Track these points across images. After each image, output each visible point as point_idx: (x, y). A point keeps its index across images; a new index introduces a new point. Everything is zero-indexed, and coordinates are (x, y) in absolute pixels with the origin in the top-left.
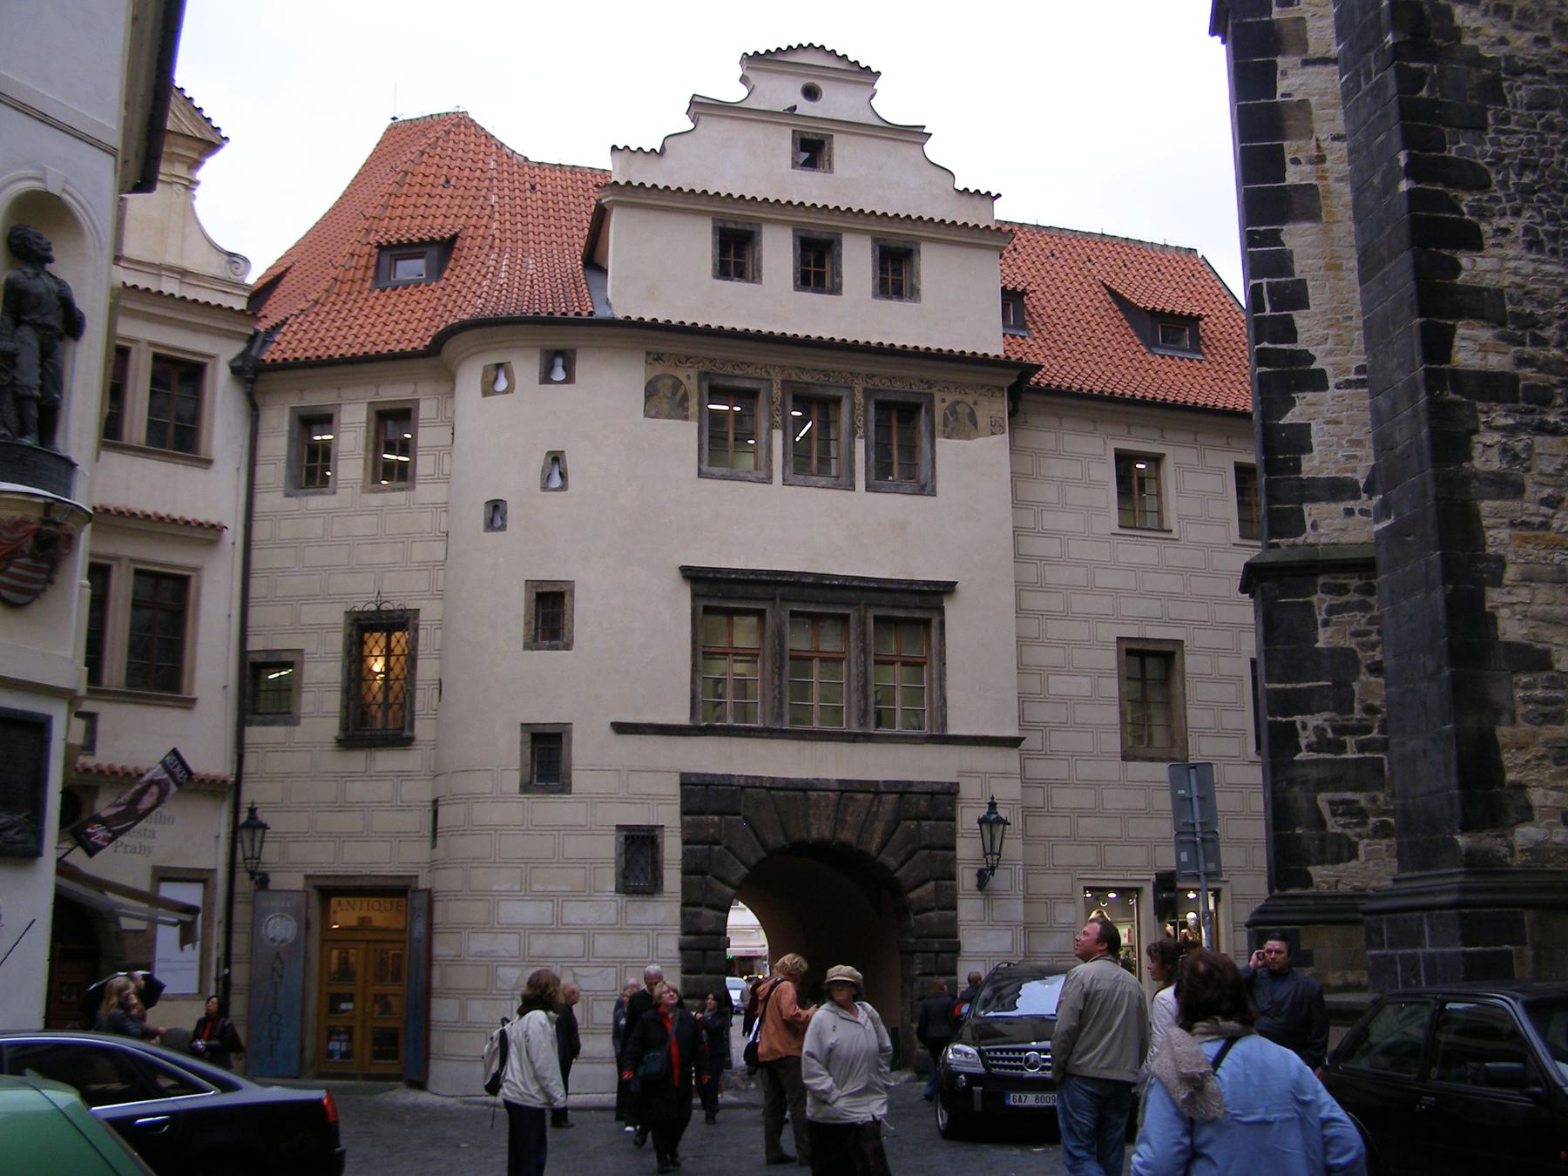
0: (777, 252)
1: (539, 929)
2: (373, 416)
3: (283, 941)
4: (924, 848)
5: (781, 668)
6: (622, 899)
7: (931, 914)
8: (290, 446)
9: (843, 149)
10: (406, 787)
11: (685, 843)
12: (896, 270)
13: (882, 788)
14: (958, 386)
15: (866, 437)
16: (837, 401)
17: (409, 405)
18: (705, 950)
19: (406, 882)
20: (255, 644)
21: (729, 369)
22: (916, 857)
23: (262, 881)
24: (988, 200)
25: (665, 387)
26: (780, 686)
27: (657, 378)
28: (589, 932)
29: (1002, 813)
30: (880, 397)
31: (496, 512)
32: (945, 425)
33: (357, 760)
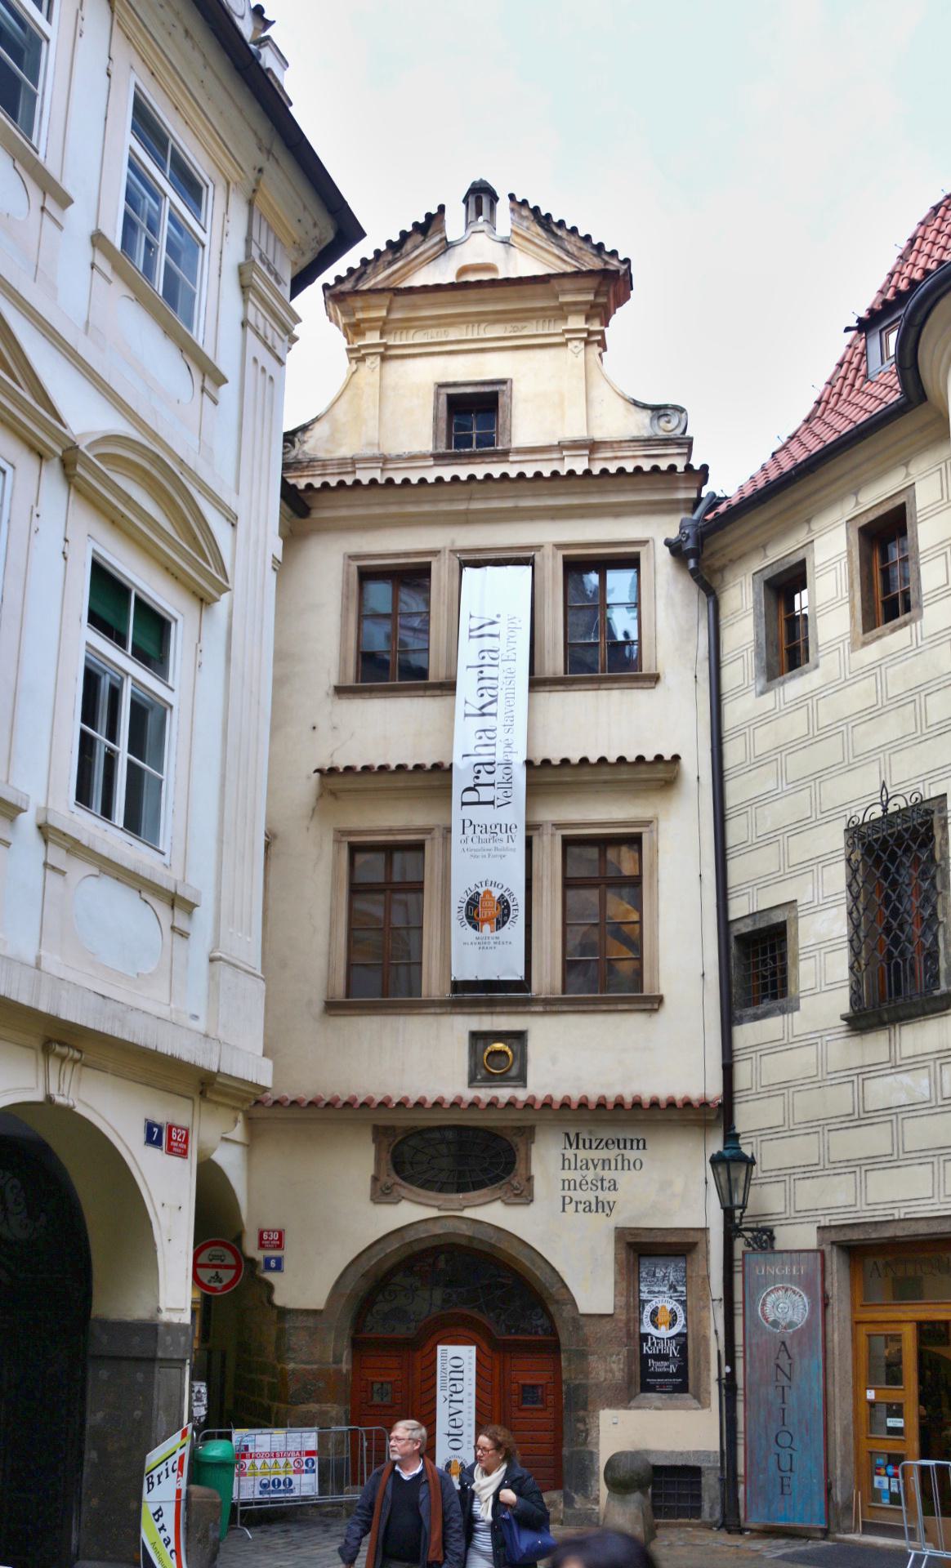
20: (739, 908)
33: (875, 1046)
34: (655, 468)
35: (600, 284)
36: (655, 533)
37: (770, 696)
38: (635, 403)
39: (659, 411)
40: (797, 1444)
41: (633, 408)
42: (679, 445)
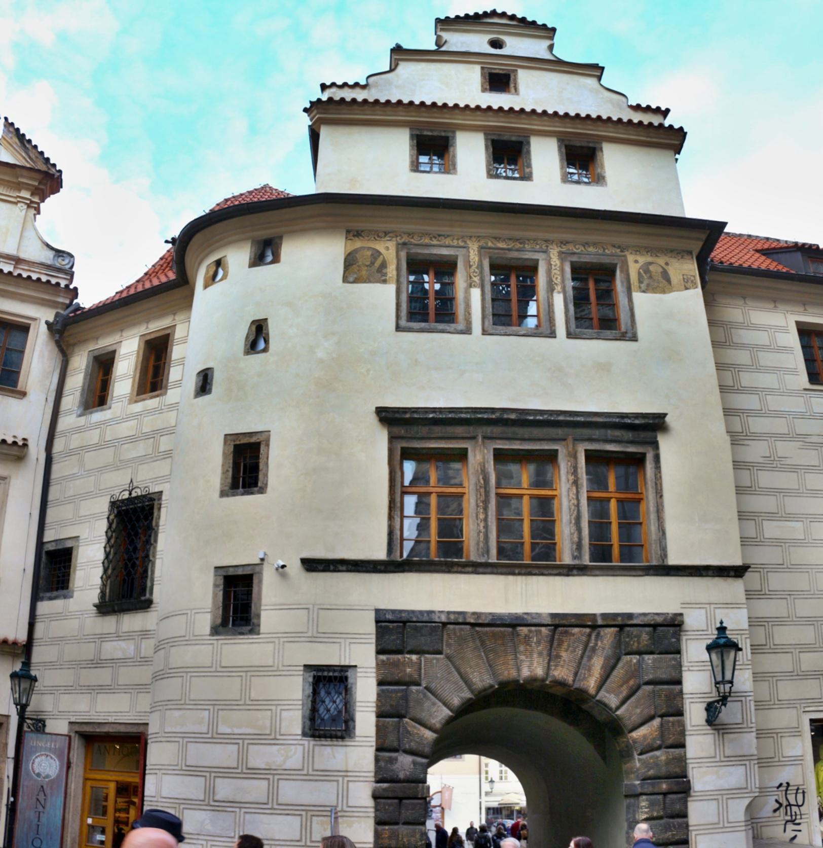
1: (225, 772)
3: (47, 776)
4: (648, 683)
5: (486, 502)
6: (309, 743)
7: (658, 753)
8: (85, 379)
11: (380, 683)
13: (600, 622)
14: (649, 250)
15: (564, 291)
18: (401, 799)
22: (639, 693)
26: (486, 520)
30: (575, 259)
32: (640, 282)
34: (48, 282)
35: (43, 179)
36: (40, 316)
37: (83, 418)
38: (48, 245)
39: (59, 253)
41: (45, 247)
42: (66, 274)
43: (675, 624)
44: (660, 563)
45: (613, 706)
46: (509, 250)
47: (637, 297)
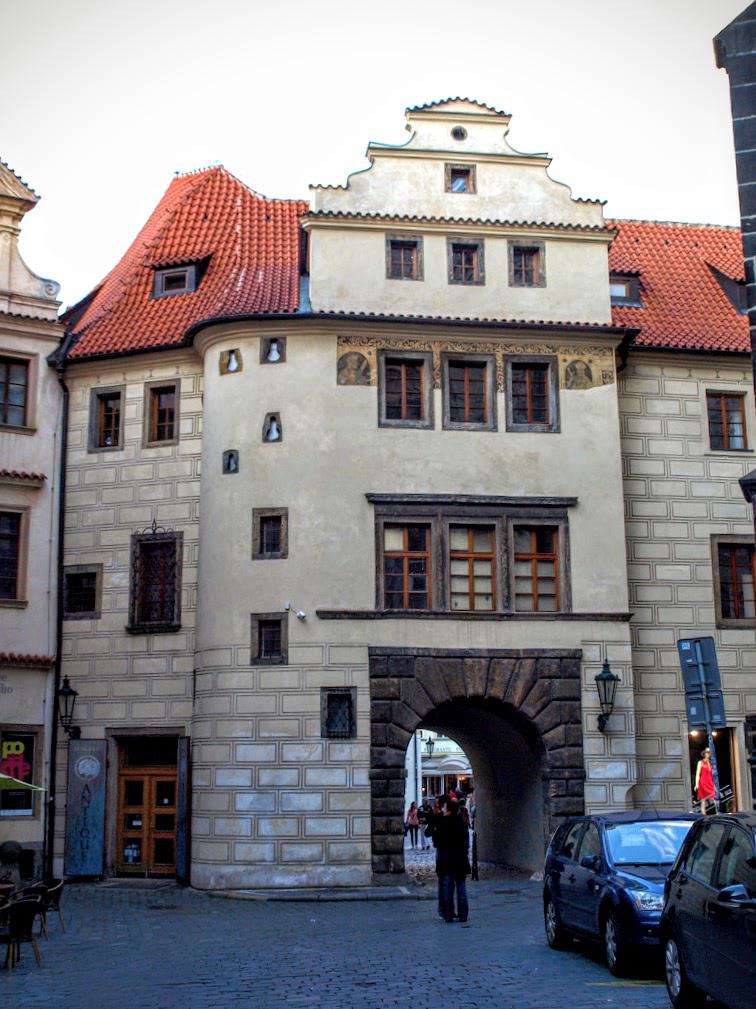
0: (435, 254)
1: (267, 765)
2: (149, 393)
3: (91, 776)
7: (562, 750)
9: (483, 173)
10: (176, 661)
11: (373, 699)
12: (525, 260)
13: (522, 655)
15: (506, 390)
16: (483, 365)
17: (173, 384)
18: (388, 779)
19: (175, 732)
20: (69, 561)
21: (400, 346)
23: (75, 733)
24: (598, 207)
25: (352, 361)
27: (346, 356)
28: (301, 766)
29: (614, 672)
30: (515, 360)
31: (231, 462)
32: (567, 379)
33: (140, 643)
40: (91, 836)
43: (576, 656)
44: (566, 612)
45: (531, 715)
46: (464, 354)
47: (563, 392)
